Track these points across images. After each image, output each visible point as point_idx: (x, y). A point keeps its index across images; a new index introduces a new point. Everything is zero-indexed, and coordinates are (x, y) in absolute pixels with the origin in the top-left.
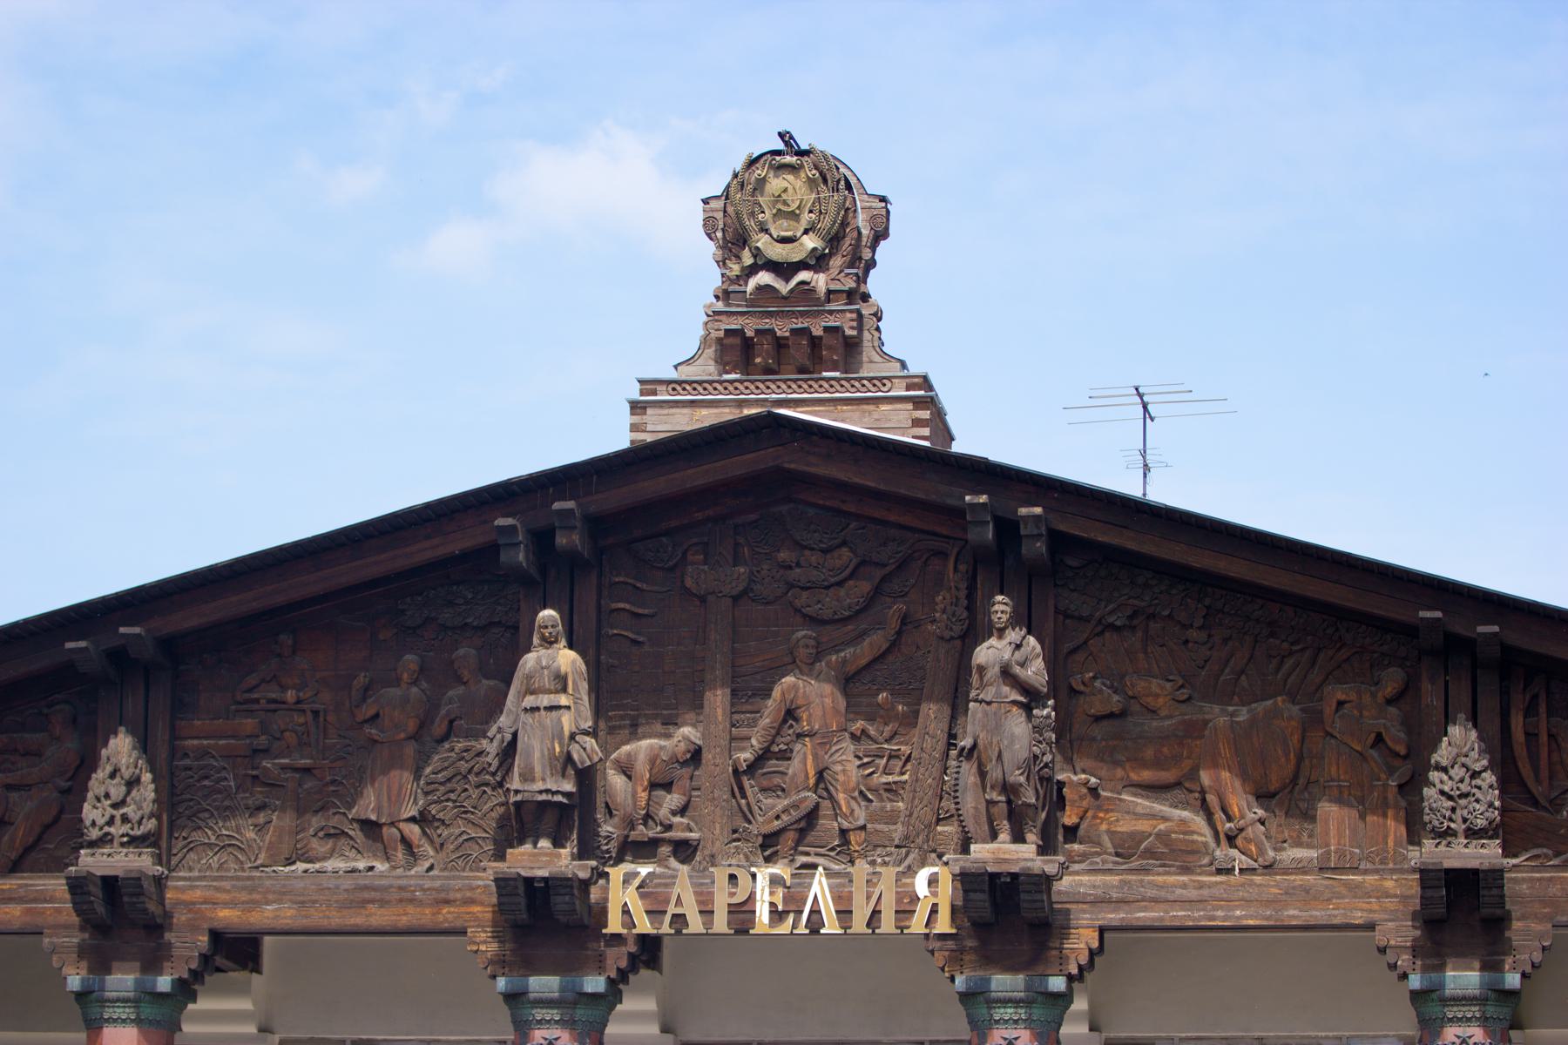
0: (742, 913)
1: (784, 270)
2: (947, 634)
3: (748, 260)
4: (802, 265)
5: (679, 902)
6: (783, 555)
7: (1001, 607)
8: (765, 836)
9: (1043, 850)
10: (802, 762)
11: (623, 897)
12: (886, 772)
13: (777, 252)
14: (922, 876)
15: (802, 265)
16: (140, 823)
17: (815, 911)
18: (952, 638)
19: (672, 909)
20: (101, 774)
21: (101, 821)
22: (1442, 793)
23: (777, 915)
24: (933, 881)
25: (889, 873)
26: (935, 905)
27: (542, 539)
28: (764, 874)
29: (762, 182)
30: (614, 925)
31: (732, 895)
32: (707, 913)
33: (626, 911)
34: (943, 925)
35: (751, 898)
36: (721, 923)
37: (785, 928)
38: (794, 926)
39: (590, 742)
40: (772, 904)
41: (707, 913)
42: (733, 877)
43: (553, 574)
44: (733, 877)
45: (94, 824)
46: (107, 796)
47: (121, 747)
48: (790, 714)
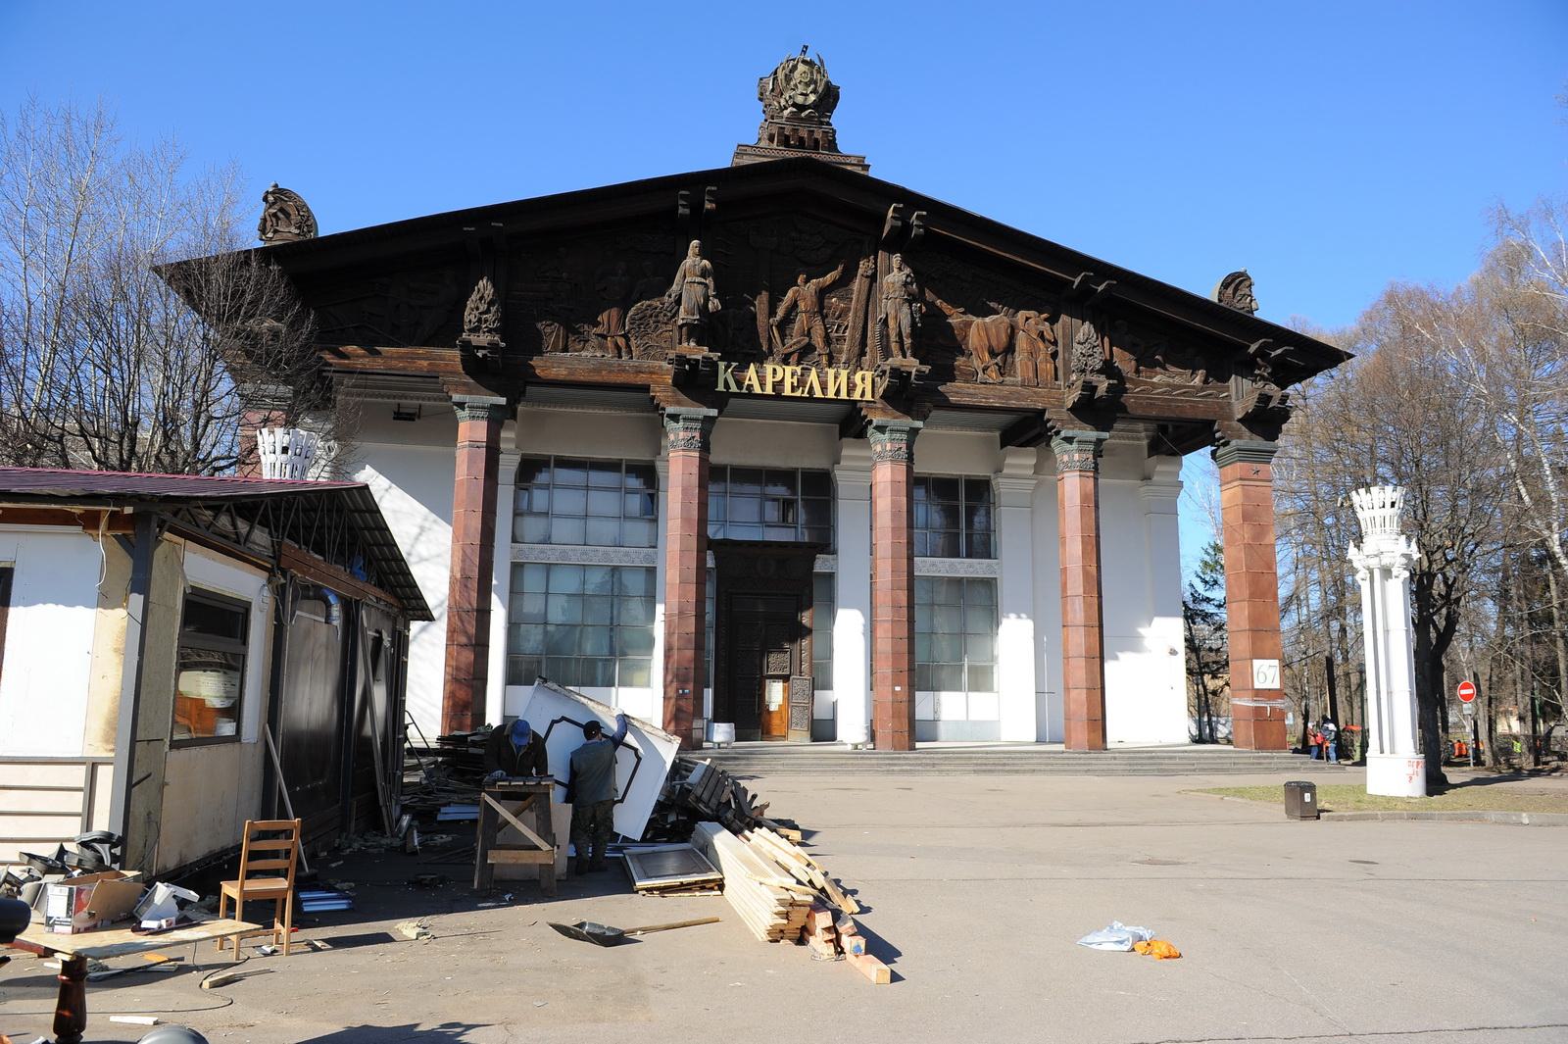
0: (778, 385)
1: (801, 108)
2: (865, 274)
3: (783, 103)
4: (809, 107)
5: (750, 380)
6: (793, 234)
7: (896, 259)
8: (786, 355)
9: (920, 364)
10: (801, 321)
11: (725, 375)
12: (836, 332)
13: (800, 100)
14: (859, 375)
15: (809, 107)
16: (494, 322)
17: (811, 387)
18: (867, 277)
19: (747, 382)
20: (474, 296)
21: (474, 320)
22: (1081, 353)
23: (793, 389)
24: (863, 379)
25: (844, 373)
26: (864, 388)
27: (696, 207)
28: (789, 369)
29: (795, 67)
30: (721, 388)
31: (774, 377)
32: (762, 385)
33: (727, 385)
34: (868, 397)
35: (783, 378)
36: (769, 390)
37: (798, 394)
38: (803, 392)
39: (716, 301)
40: (792, 383)
41: (762, 385)
42: (774, 370)
43: (699, 225)
44: (774, 370)
45: (470, 321)
46: (477, 309)
47: (485, 287)
48: (794, 305)
